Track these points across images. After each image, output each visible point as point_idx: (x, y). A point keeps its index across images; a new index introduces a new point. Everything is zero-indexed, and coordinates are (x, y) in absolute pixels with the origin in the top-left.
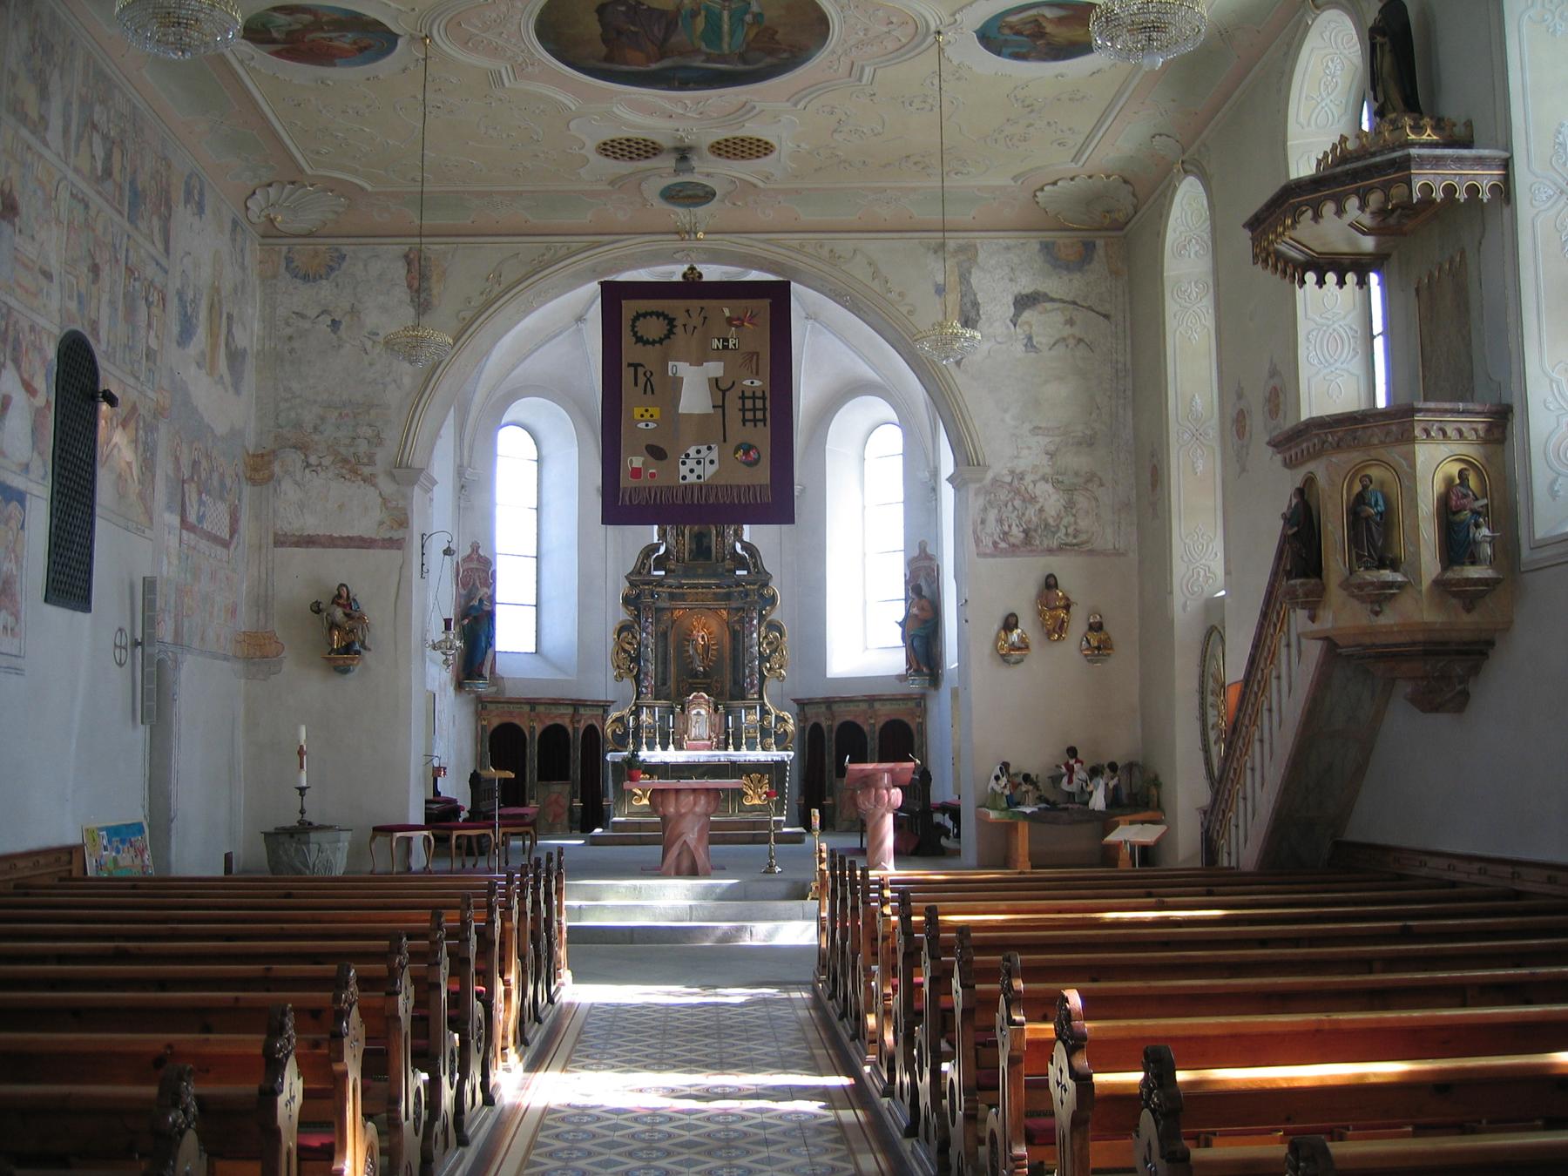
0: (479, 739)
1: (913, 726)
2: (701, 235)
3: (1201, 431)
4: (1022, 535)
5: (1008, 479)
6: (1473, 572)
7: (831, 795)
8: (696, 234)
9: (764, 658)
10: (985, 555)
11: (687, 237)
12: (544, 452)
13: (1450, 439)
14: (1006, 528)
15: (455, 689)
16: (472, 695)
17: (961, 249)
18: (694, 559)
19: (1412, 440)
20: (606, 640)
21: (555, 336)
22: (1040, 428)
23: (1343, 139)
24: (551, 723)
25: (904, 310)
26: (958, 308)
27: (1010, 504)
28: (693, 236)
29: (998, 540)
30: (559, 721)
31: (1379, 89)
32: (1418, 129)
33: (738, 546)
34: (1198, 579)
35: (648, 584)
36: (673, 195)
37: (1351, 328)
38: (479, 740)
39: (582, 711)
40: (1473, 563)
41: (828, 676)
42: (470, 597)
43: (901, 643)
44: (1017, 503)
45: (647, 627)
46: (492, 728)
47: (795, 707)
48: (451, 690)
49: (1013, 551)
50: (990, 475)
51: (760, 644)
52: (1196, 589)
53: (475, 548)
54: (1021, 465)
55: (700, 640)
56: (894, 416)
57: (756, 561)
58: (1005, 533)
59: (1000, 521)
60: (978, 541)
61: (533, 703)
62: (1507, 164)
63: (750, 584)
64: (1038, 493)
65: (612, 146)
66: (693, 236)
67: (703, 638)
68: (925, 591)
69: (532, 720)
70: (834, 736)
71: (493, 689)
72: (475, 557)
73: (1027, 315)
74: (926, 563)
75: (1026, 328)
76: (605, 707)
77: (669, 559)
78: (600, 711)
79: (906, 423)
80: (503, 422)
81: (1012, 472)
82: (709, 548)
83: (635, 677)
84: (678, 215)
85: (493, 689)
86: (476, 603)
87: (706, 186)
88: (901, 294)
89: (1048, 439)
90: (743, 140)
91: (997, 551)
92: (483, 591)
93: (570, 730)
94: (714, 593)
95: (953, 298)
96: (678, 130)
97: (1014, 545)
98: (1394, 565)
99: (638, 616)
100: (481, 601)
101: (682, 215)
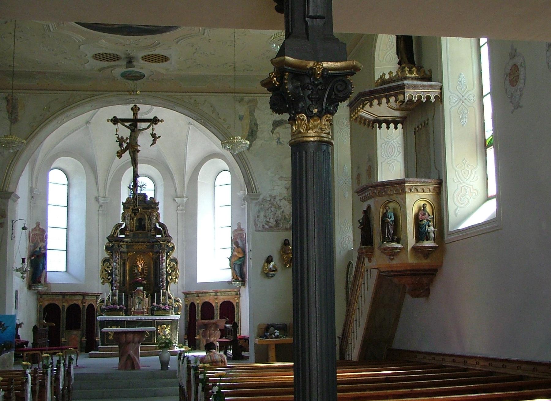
1: (235, 304)
2: (138, 92)
3: (347, 180)
4: (275, 223)
5: (269, 199)
6: (426, 244)
8: (136, 92)
9: (168, 274)
10: (259, 231)
11: (132, 93)
12: (70, 182)
13: (419, 192)
14: (268, 220)
15: (28, 289)
17: (250, 101)
18: (137, 230)
19: (404, 193)
20: (98, 266)
21: (76, 130)
22: (283, 177)
23: (384, 74)
25: (226, 126)
26: (249, 126)
27: (270, 209)
28: (135, 92)
29: (264, 224)
30: (76, 302)
31: (399, 54)
32: (410, 72)
34: (345, 242)
35: (117, 241)
36: (126, 76)
37: (398, 143)
38: (38, 311)
39: (87, 298)
40: (427, 240)
41: (199, 281)
42: (35, 246)
43: (229, 267)
44: (273, 209)
45: (116, 260)
46: (43, 307)
47: (183, 296)
48: (26, 289)
49: (271, 229)
50: (261, 197)
51: (167, 268)
52: (345, 246)
53: (38, 224)
54: (274, 193)
55: (140, 266)
56: (228, 168)
57: (165, 231)
58: (268, 222)
59: (265, 216)
60: (256, 225)
61: (64, 295)
62: (441, 88)
63: (162, 241)
64: (281, 205)
65: (99, 56)
66: (135, 92)
67: (141, 265)
68: (240, 244)
70: (200, 308)
71: (45, 288)
72: (38, 228)
73: (278, 129)
74: (241, 232)
75: (278, 135)
76: (97, 296)
77: (126, 230)
78: (95, 298)
79: (231, 171)
80: (52, 168)
81: (271, 196)
82: (145, 225)
83: (110, 282)
84: (129, 83)
85: (45, 288)
86: (38, 249)
87: (141, 72)
88: (224, 120)
89: (287, 182)
90: (155, 55)
91: (264, 229)
92: (41, 244)
93: (81, 307)
95: (246, 121)
96: (127, 51)
97: (271, 227)
98: (398, 241)
99: (112, 255)
100: (40, 248)
101: (130, 84)
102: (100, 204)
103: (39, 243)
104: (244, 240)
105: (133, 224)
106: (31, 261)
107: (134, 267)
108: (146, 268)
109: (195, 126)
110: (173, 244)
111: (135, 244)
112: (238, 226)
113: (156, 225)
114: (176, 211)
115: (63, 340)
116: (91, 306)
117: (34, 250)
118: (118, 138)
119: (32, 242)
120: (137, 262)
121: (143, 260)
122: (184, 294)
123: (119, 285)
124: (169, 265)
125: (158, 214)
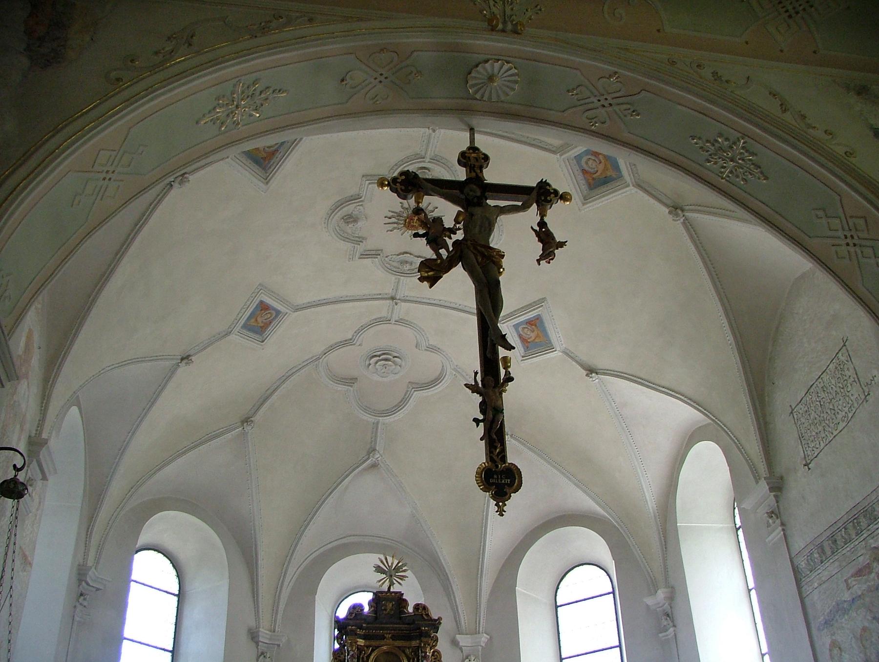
12: (188, 587)
80: (142, 540)
102: (260, 651)
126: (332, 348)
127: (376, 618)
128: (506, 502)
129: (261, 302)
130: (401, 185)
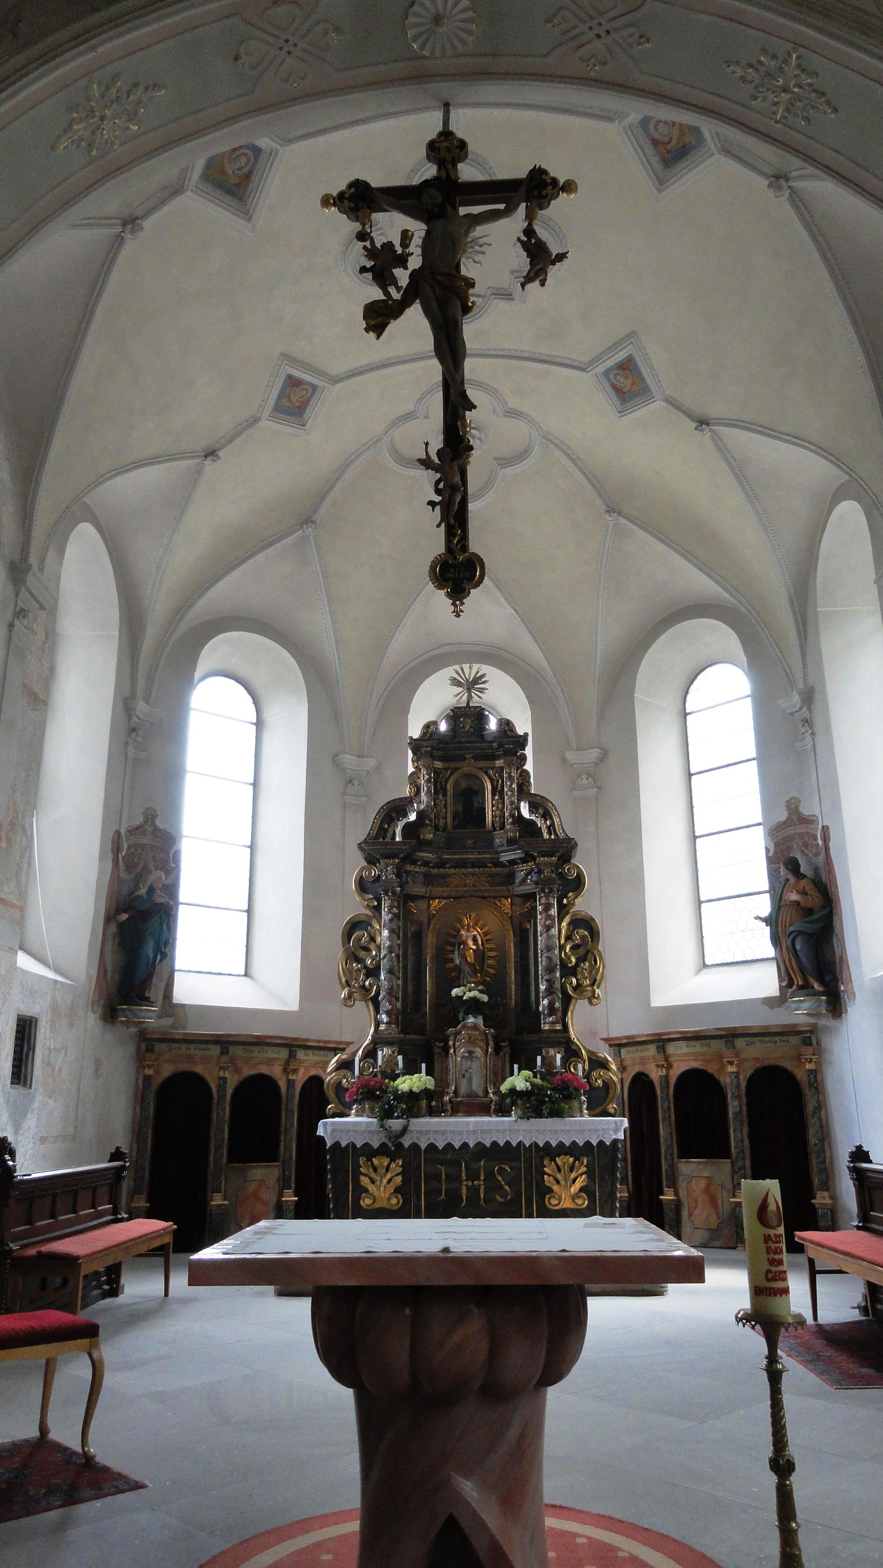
0: (139, 1098)
1: (800, 1075)
7: (674, 1185)
9: (568, 971)
16: (133, 1030)
24: (253, 1072)
30: (264, 1070)
33: (525, 810)
38: (140, 1098)
39: (301, 1054)
43: (770, 951)
46: (156, 1084)
51: (562, 948)
55: (470, 943)
61: (224, 1043)
63: (544, 856)
69: (222, 1068)
71: (167, 1022)
74: (800, 829)
83: (372, 999)
85: (167, 1022)
86: (143, 891)
92: (156, 876)
93: (282, 1084)
94: (491, 875)
103: (150, 873)
104: (817, 855)
105: (446, 807)
106: (121, 926)
107: (449, 948)
108: (491, 950)
109: (624, 517)
110: (578, 867)
111: (452, 870)
112: (789, 807)
113: (518, 809)
114: (571, 791)
115: (217, 1200)
116: (315, 1082)
117: (133, 892)
118: (371, 253)
119: (128, 868)
120: (459, 931)
121: (481, 923)
122: (611, 1046)
123: (399, 1005)
124: (568, 938)
125: (525, 775)
126: (394, 424)
127: (454, 737)
128: (464, 601)
129: (290, 377)
130: (350, 202)
